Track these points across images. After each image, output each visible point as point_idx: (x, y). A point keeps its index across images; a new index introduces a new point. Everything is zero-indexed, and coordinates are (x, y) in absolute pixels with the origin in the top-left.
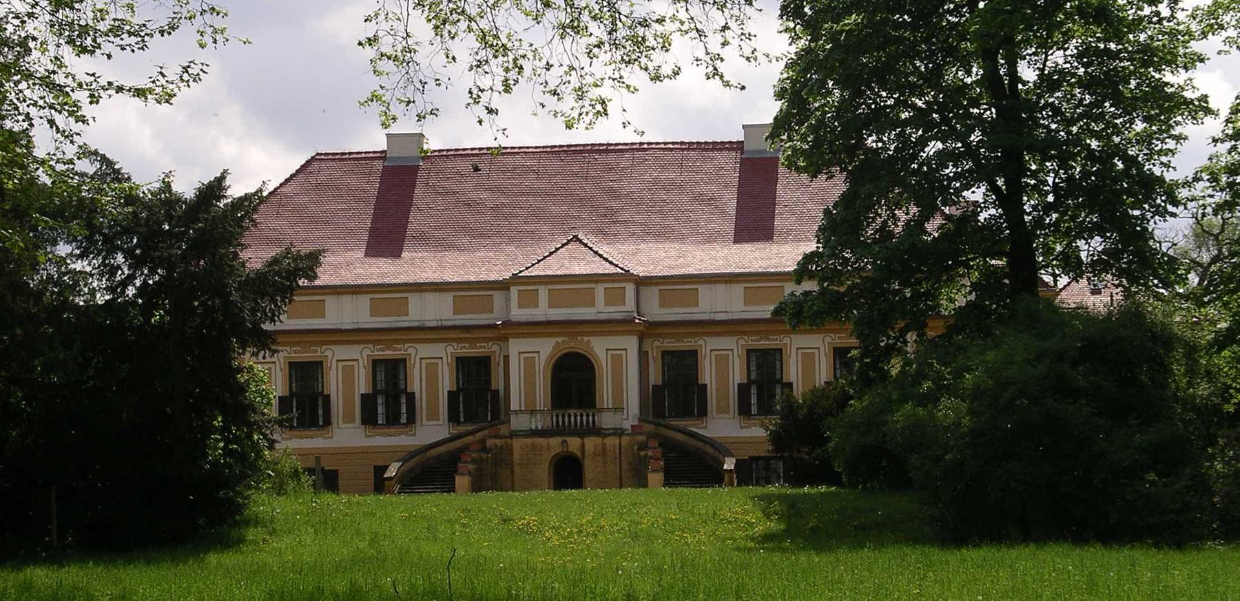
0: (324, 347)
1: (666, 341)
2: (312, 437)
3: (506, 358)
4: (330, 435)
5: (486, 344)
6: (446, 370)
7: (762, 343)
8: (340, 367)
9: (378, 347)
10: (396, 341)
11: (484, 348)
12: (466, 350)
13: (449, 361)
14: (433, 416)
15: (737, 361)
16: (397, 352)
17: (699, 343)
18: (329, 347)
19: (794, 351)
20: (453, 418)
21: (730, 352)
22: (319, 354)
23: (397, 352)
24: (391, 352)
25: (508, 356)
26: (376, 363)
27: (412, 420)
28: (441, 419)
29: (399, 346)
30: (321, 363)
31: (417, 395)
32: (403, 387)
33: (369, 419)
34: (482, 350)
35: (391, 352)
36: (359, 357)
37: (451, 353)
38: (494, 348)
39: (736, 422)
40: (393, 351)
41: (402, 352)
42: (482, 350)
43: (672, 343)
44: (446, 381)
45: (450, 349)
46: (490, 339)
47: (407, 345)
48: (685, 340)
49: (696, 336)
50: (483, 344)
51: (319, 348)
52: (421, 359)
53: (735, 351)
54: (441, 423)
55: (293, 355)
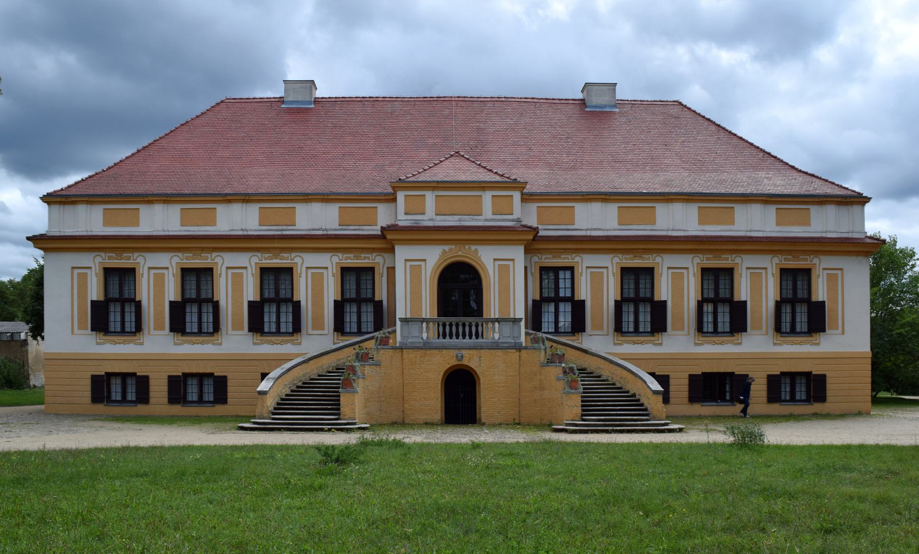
0: (214, 254)
1: (544, 257)
2: (202, 343)
3: (391, 270)
4: (220, 341)
5: (370, 255)
7: (635, 261)
9: (266, 255)
11: (369, 259)
12: (352, 261)
13: (334, 271)
14: (318, 324)
15: (611, 279)
16: (285, 261)
19: (665, 269)
20: (339, 327)
21: (605, 270)
22: (209, 261)
23: (285, 261)
24: (278, 261)
25: (394, 268)
27: (297, 328)
28: (326, 328)
29: (286, 255)
30: (211, 270)
31: (303, 304)
33: (256, 325)
34: (366, 261)
35: (278, 261)
36: (247, 264)
37: (337, 263)
39: (610, 338)
40: (281, 259)
41: (289, 261)
42: (366, 261)
43: (549, 258)
44: (331, 292)
46: (373, 250)
47: (293, 255)
48: (562, 256)
49: (573, 253)
50: (367, 255)
51: (209, 255)
52: (307, 268)
53: (610, 268)
54: (326, 332)
55: (185, 261)
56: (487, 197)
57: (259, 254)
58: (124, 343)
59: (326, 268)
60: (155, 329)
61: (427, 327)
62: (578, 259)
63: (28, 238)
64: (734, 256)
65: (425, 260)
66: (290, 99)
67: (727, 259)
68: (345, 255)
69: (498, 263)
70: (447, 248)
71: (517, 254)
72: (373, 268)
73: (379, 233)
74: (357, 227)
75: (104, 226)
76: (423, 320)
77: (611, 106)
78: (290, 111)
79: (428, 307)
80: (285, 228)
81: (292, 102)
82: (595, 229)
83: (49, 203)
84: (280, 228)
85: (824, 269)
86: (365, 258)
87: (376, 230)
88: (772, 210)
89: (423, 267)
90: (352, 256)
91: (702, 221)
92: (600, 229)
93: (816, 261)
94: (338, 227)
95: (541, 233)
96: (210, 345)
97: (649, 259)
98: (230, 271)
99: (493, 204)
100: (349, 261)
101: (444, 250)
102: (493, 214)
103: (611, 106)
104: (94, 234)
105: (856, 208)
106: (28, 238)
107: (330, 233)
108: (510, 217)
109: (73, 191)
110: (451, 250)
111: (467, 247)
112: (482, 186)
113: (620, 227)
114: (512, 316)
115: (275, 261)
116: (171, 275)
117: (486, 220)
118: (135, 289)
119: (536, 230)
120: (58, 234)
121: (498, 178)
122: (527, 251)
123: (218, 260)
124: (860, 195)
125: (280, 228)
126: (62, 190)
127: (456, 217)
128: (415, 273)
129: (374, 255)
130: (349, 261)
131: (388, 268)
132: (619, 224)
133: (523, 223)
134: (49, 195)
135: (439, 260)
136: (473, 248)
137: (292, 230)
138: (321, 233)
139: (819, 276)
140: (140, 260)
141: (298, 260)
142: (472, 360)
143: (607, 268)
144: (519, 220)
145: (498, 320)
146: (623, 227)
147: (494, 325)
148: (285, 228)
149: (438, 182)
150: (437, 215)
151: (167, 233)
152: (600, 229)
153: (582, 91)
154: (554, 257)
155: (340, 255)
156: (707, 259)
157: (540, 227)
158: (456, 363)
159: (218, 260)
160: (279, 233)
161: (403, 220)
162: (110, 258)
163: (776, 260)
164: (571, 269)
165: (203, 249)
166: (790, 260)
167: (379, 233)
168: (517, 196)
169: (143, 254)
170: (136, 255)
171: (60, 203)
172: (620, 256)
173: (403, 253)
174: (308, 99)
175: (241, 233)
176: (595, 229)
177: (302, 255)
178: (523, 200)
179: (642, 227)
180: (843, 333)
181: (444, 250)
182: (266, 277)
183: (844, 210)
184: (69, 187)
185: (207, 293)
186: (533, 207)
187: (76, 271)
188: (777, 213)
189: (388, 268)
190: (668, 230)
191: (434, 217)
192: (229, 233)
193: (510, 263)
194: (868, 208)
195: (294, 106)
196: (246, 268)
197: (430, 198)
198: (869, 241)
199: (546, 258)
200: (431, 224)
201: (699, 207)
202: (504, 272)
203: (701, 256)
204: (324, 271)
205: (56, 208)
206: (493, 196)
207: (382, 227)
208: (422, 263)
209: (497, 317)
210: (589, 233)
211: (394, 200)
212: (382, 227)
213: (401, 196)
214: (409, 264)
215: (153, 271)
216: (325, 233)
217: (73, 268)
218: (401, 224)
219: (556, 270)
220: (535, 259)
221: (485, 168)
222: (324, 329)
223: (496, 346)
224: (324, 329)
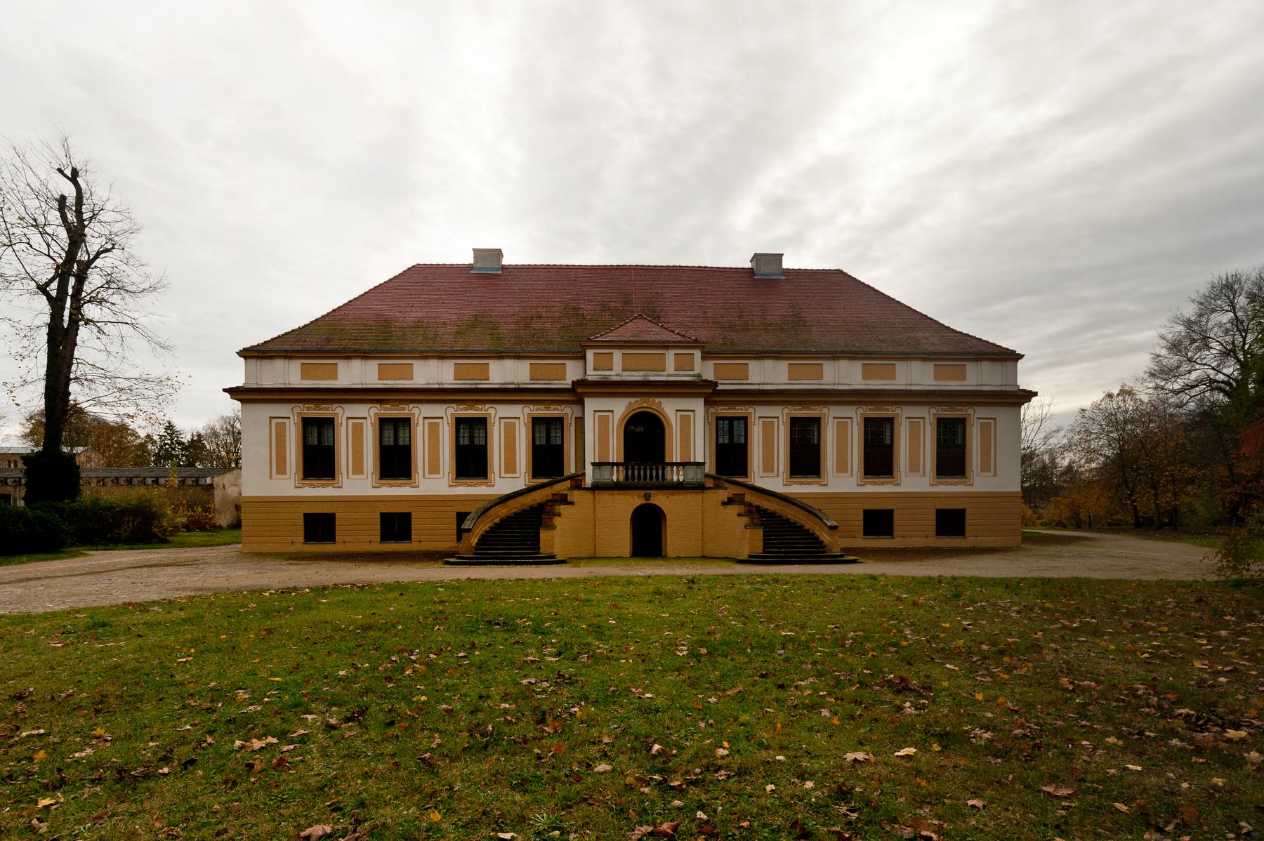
1: (720, 408)
3: (580, 421)
5: (559, 407)
6: (523, 429)
8: (502, 425)
9: (461, 407)
10: (477, 402)
11: (558, 410)
12: (541, 411)
17: (749, 411)
18: (416, 405)
21: (775, 420)
22: (406, 411)
24: (473, 412)
26: (536, 421)
29: (480, 407)
32: (560, 443)
34: (556, 412)
35: (473, 412)
37: (528, 414)
38: (568, 412)
42: (556, 412)
43: (725, 409)
45: (527, 410)
46: (562, 402)
47: (487, 406)
51: (407, 407)
52: (500, 418)
55: (383, 412)
56: (670, 355)
57: (455, 406)
58: (322, 486)
59: (519, 418)
60: (353, 474)
61: (618, 470)
62: (751, 410)
63: (225, 390)
64: (894, 407)
65: (612, 411)
66: (479, 265)
67: (888, 410)
68: (536, 407)
69: (679, 413)
70: (633, 400)
71: (698, 405)
72: (820, 418)
73: (570, 386)
74: (547, 382)
75: (302, 379)
76: (613, 464)
77: (778, 274)
78: (478, 276)
79: (615, 452)
80: (479, 382)
81: (481, 268)
82: (767, 384)
83: (245, 358)
84: (475, 382)
85: (978, 418)
86: (555, 409)
87: (567, 383)
88: (930, 366)
89: (611, 417)
90: (542, 407)
91: (865, 377)
92: (772, 384)
93: (970, 411)
94: (529, 382)
95: (720, 387)
96: (407, 487)
97: (816, 410)
98: (427, 421)
99: (676, 361)
100: (539, 412)
101: (630, 402)
102: (676, 370)
103: (778, 274)
104: (263, 386)
105: (1009, 364)
106: (225, 390)
107: (522, 386)
108: (691, 373)
109: (270, 347)
110: (636, 402)
111: (651, 399)
112: (666, 345)
113: (790, 382)
114: (692, 461)
115: (469, 412)
116: (446, 424)
117: (669, 375)
118: (334, 438)
119: (716, 384)
120: (255, 386)
121: (680, 338)
122: (706, 403)
123: (416, 411)
124: (1013, 352)
125: (475, 382)
126: (258, 345)
127: (641, 373)
128: (603, 424)
129: (563, 406)
130: (539, 412)
131: (576, 418)
132: (789, 379)
133: (704, 378)
134: (245, 350)
135: (626, 411)
136: (657, 400)
137: (562, 384)
138: (513, 386)
139: (973, 425)
140: (339, 410)
141: (491, 411)
142: (659, 499)
143: (778, 418)
144: (699, 375)
145: (678, 464)
146: (793, 382)
147: (672, 468)
148: (479, 382)
149: (625, 342)
150: (623, 370)
151: (365, 386)
152: (772, 384)
153: (751, 261)
154: (729, 409)
155: (531, 407)
156: (870, 410)
157: (719, 382)
158: (644, 502)
159: (416, 411)
160: (474, 386)
161: (592, 375)
162: (308, 409)
163: (933, 411)
164: (745, 419)
165: (401, 401)
166: (946, 410)
167: (570, 386)
168: (697, 354)
169: (342, 405)
170: (335, 406)
171: (257, 358)
172: (790, 407)
173: (591, 405)
174: (496, 266)
175: (437, 386)
176: (767, 384)
177: (495, 406)
178: (703, 358)
179: (810, 382)
180: (995, 475)
181: (630, 402)
182: (537, 427)
183: (997, 367)
184: (266, 342)
185: (404, 441)
186: (710, 364)
187: (274, 421)
188: (935, 369)
189: (576, 418)
190: (834, 384)
191: (621, 373)
192: (425, 386)
193: (691, 414)
194: (1020, 364)
195: (483, 272)
196: (442, 418)
197: (617, 355)
198: (1021, 393)
199: (722, 410)
200: (617, 379)
201: (863, 364)
202: (685, 422)
203: (864, 407)
204: (517, 421)
205: (253, 362)
206: (675, 354)
207: (573, 382)
208: (610, 414)
209: (678, 461)
210: (761, 387)
211: (584, 358)
212: (573, 382)
213: (590, 354)
214: (597, 414)
215: (351, 421)
216: (517, 386)
217: (271, 418)
218: (590, 378)
219: (731, 420)
220: (712, 410)
221: (667, 329)
222: (515, 473)
223: (680, 487)
224: (515, 473)
